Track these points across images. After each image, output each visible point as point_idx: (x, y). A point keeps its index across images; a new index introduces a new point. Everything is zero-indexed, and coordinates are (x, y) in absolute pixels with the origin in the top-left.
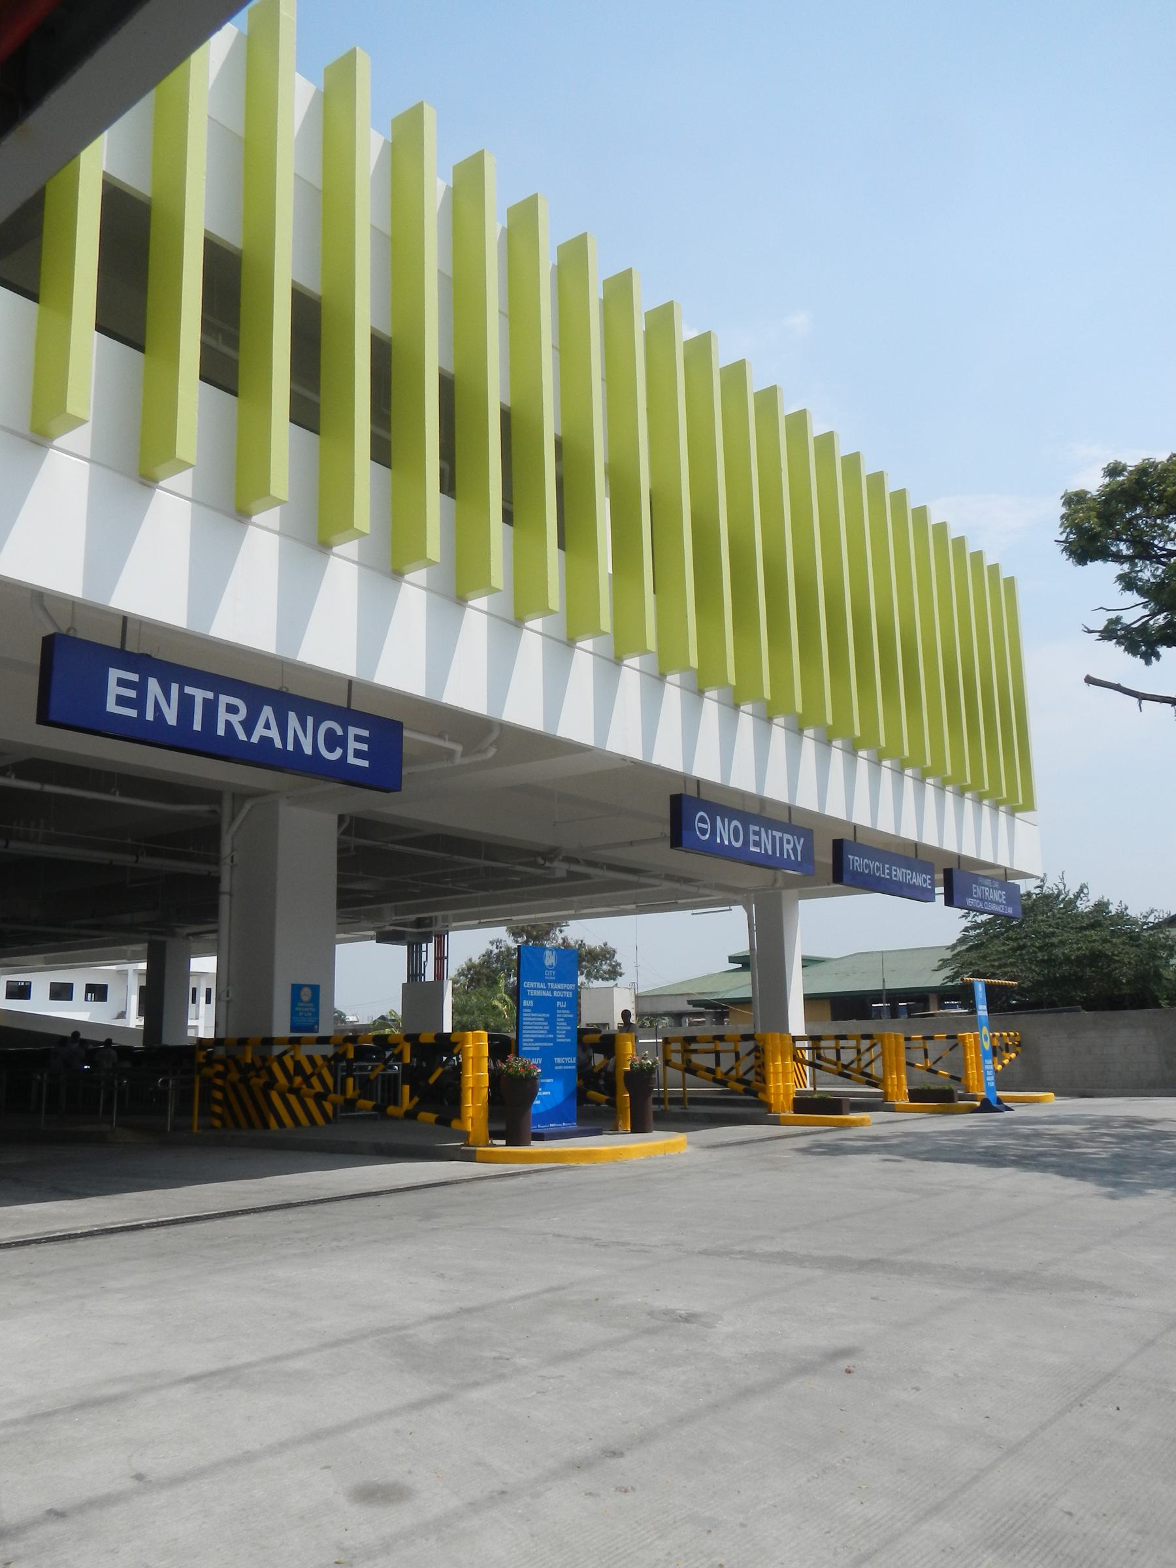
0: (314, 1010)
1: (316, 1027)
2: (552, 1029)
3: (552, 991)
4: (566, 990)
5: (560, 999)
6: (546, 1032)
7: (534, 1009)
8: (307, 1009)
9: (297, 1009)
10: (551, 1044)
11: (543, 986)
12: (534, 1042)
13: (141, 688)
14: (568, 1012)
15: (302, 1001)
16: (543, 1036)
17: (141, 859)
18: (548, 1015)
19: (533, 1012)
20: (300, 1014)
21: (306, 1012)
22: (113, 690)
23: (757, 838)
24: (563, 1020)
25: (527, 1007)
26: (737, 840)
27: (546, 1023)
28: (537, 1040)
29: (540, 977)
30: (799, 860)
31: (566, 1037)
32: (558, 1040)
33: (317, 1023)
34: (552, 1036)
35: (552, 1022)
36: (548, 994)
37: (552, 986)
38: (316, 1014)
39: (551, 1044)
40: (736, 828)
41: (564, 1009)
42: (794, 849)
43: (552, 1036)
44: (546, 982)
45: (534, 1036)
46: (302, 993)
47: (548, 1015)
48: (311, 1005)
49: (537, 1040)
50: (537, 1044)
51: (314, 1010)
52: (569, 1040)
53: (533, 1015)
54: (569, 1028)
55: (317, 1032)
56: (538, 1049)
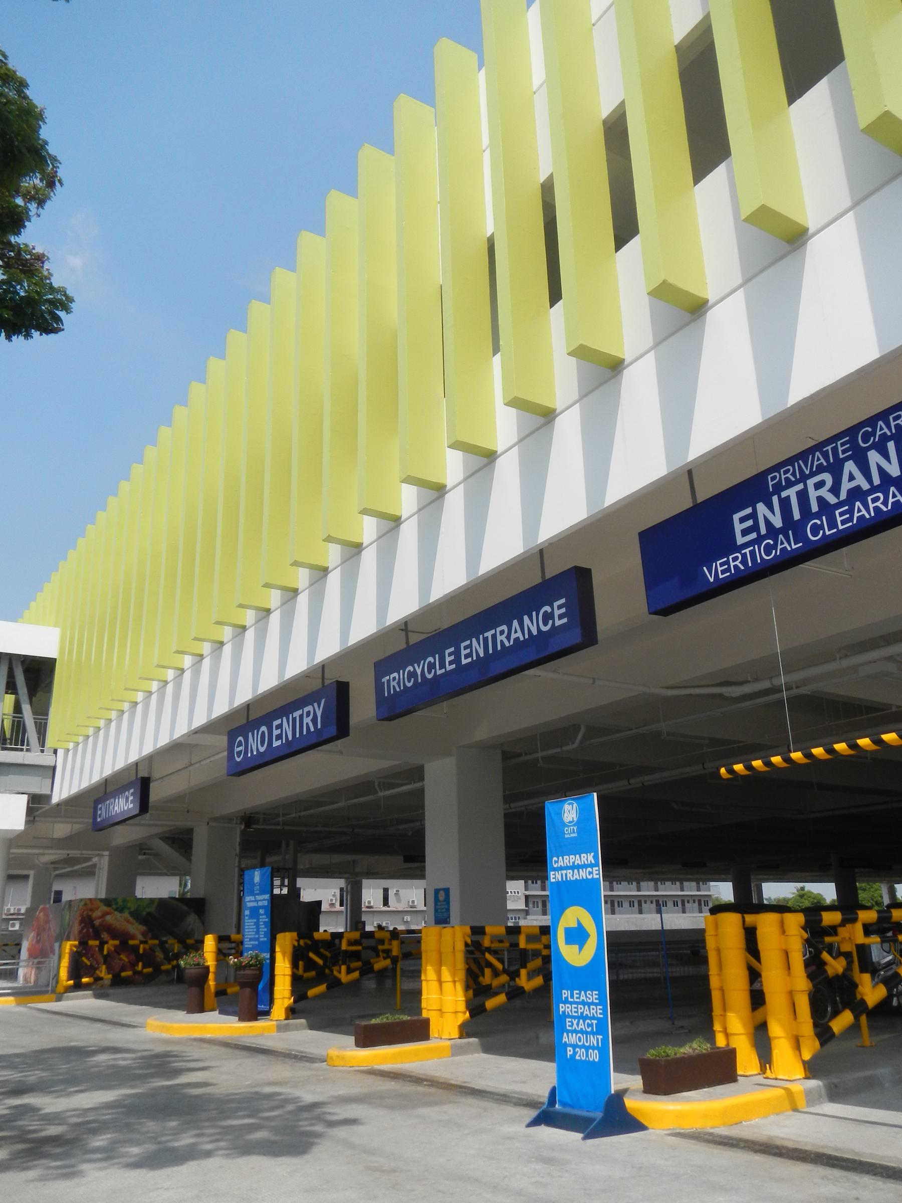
0: (446, 907)
1: (448, 920)
2: (258, 932)
3: (257, 901)
4: (264, 900)
5: (262, 907)
6: (254, 933)
7: (251, 917)
8: (442, 907)
9: (438, 907)
10: (257, 943)
11: (252, 898)
12: (250, 941)
13: (101, 809)
14: (265, 917)
15: (440, 901)
16: (252, 936)
17: (705, 766)
18: (255, 920)
19: (249, 919)
20: (439, 910)
21: (443, 909)
22: (99, 812)
23: (279, 731)
24: (253, 924)
25: (247, 916)
26: (262, 744)
27: (255, 927)
28: (251, 939)
29: (252, 893)
30: (319, 727)
31: (264, 937)
32: (262, 939)
33: (449, 917)
34: (257, 936)
35: (257, 924)
36: (255, 904)
37: (258, 898)
38: (448, 910)
39: (257, 943)
40: (263, 733)
41: (262, 915)
42: (314, 720)
43: (257, 936)
44: (255, 895)
45: (249, 936)
46: (440, 895)
47: (255, 920)
48: (445, 903)
49: (251, 939)
50: (252, 943)
51: (446, 907)
52: (266, 939)
53: (250, 921)
54: (266, 930)
55: (449, 923)
56: (251, 946)
